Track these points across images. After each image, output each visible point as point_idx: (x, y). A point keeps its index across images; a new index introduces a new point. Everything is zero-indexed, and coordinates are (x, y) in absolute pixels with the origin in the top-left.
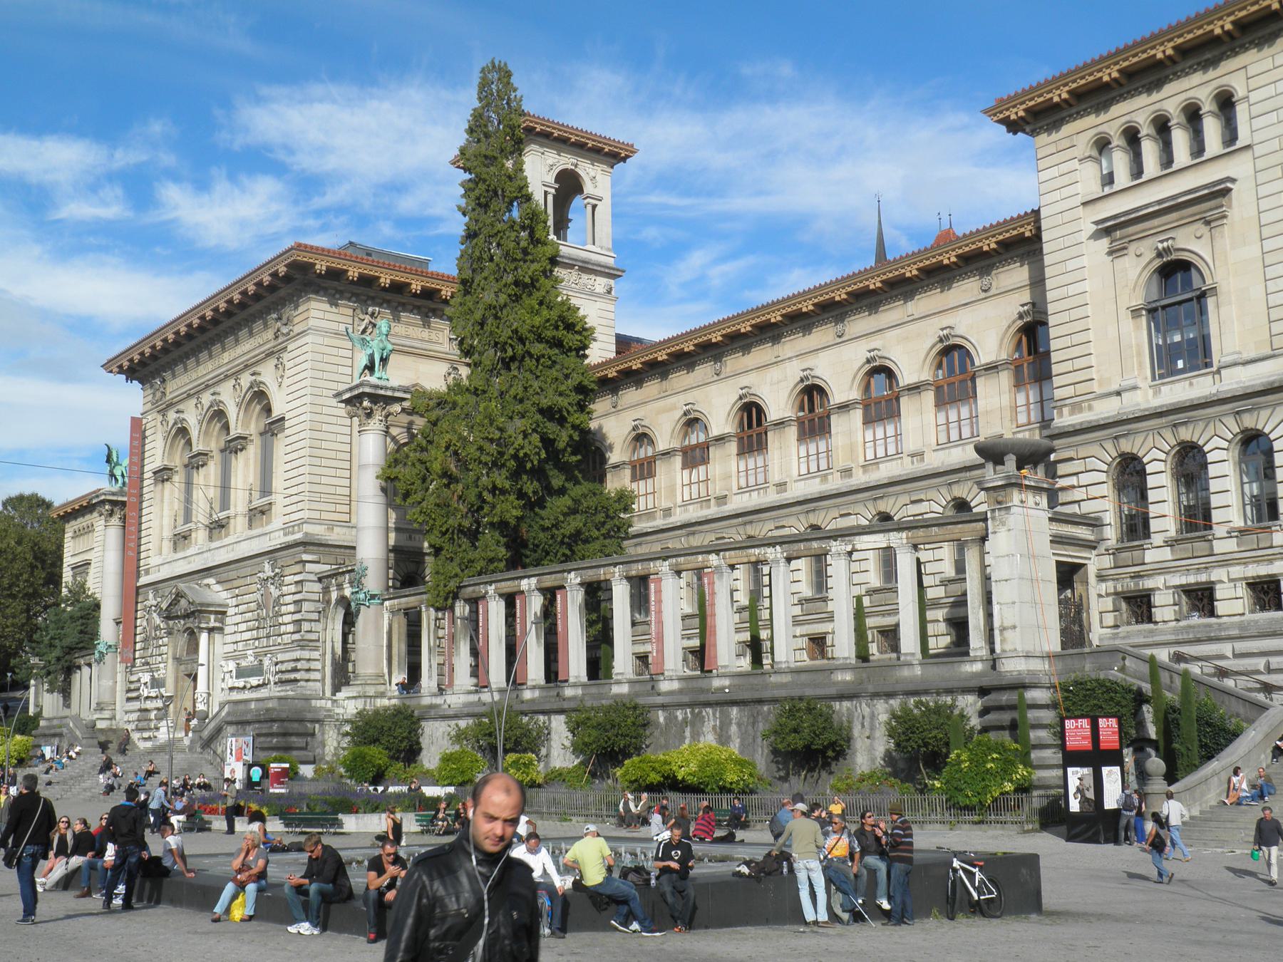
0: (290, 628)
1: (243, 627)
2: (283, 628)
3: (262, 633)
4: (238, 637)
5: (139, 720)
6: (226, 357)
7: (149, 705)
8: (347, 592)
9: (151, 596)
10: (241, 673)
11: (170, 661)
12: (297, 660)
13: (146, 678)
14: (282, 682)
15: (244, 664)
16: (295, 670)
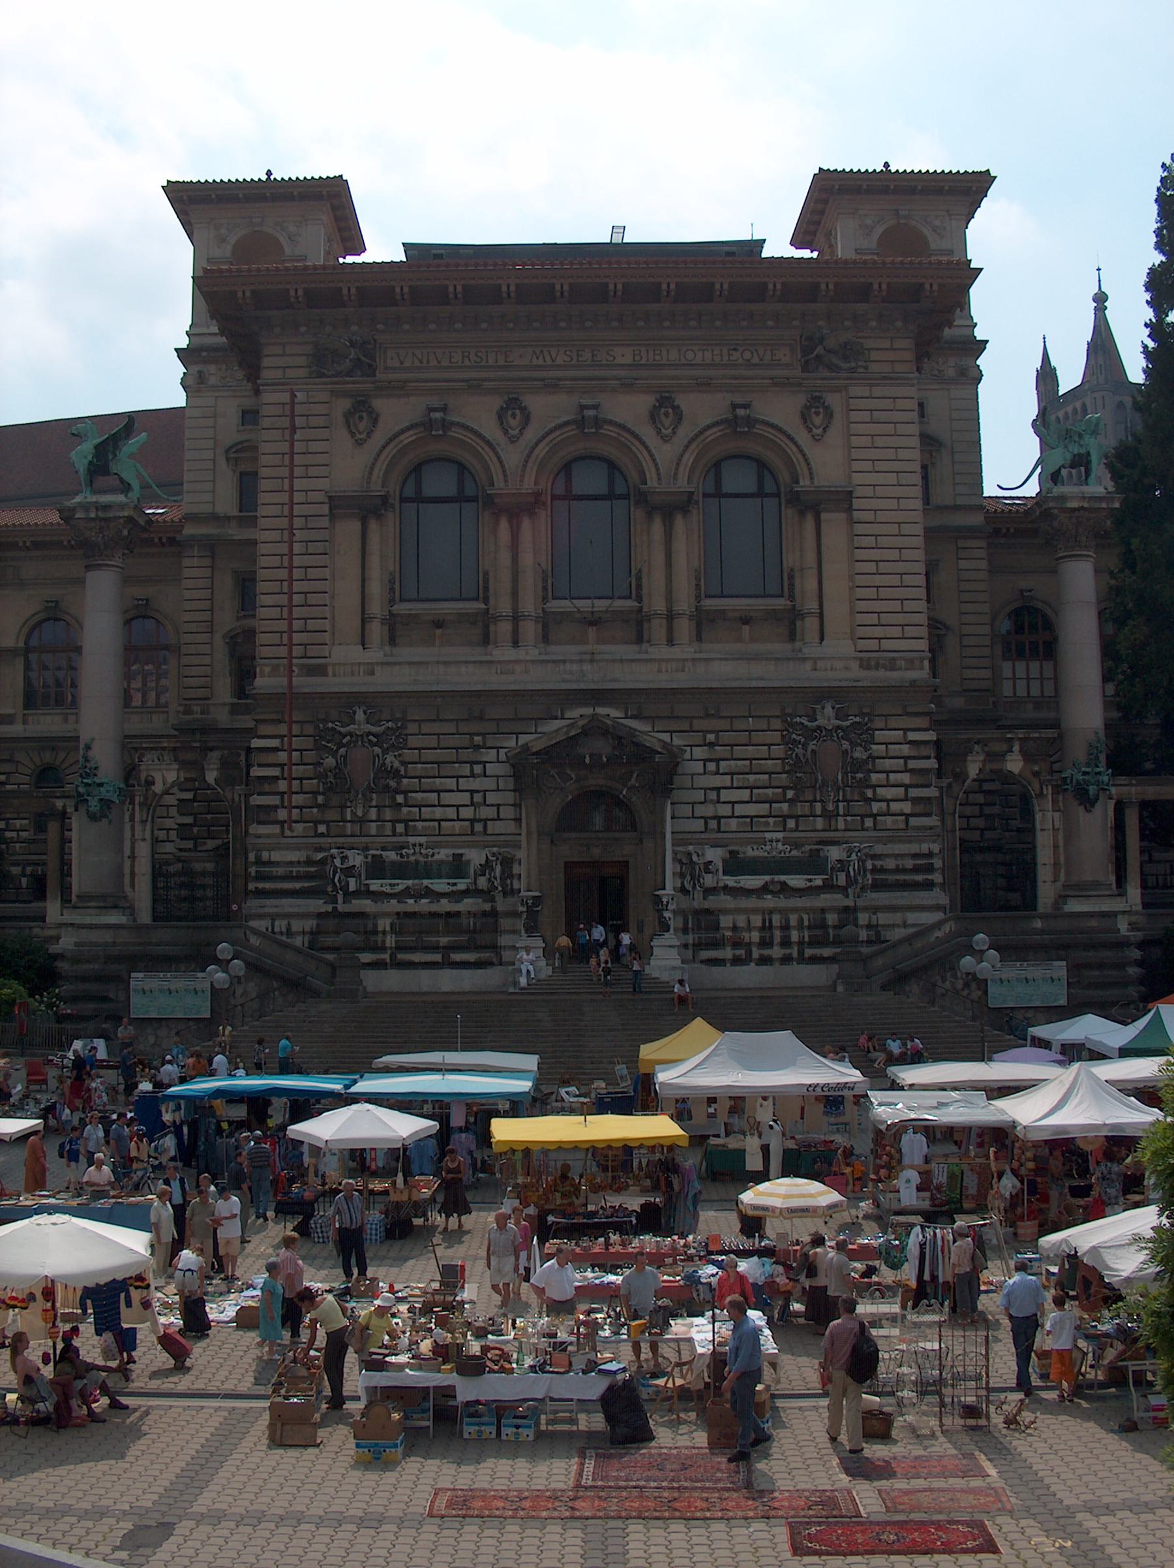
0: (907, 807)
1: (745, 794)
2: (876, 807)
3: (801, 809)
4: (725, 810)
5: (315, 933)
6: (624, 356)
7: (366, 905)
8: (1014, 764)
9: (360, 715)
10: (736, 864)
11: (535, 836)
12: (930, 855)
13: (356, 859)
14: (877, 886)
15: (750, 852)
16: (930, 869)
